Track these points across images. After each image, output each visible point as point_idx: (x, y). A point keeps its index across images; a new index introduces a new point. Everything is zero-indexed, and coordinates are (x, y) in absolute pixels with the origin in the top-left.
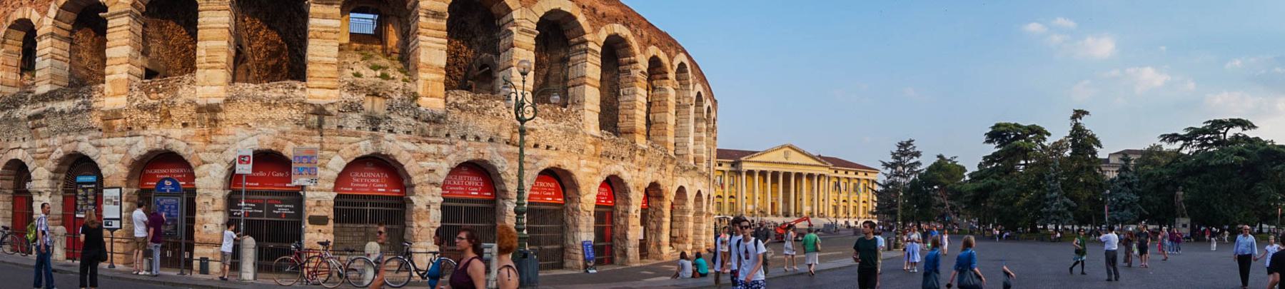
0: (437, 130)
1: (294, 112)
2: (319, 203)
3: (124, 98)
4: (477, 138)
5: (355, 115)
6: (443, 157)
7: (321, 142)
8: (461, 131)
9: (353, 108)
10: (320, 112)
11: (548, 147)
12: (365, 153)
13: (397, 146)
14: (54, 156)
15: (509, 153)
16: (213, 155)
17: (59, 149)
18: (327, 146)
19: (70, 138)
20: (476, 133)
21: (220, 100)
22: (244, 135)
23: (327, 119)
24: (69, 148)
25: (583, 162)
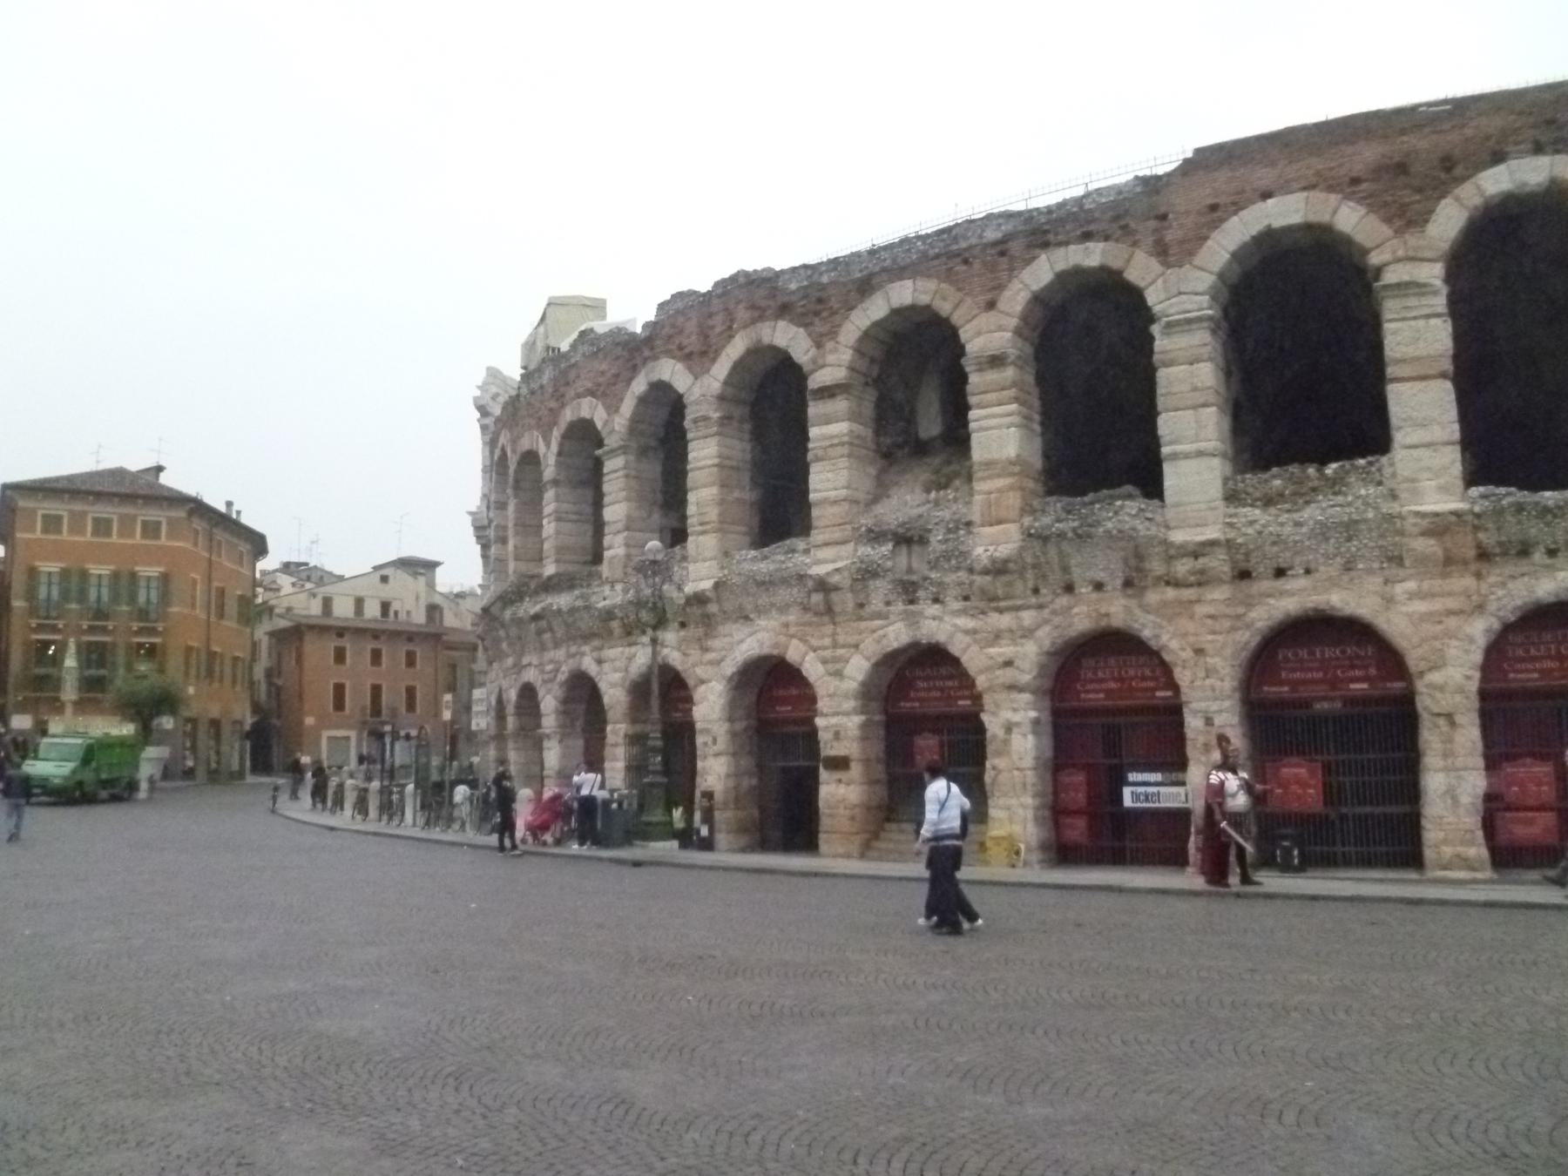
0: (1010, 584)
2: (837, 736)
4: (1099, 586)
5: (878, 583)
6: (1028, 633)
7: (834, 634)
8: (1056, 577)
9: (867, 573)
10: (823, 586)
11: (1280, 573)
12: (895, 645)
13: (942, 624)
14: (562, 677)
15: (1165, 604)
16: (709, 668)
17: (564, 668)
18: (841, 639)
19: (573, 649)
20: (1091, 574)
21: (707, 585)
23: (834, 597)
25: (1399, 589)
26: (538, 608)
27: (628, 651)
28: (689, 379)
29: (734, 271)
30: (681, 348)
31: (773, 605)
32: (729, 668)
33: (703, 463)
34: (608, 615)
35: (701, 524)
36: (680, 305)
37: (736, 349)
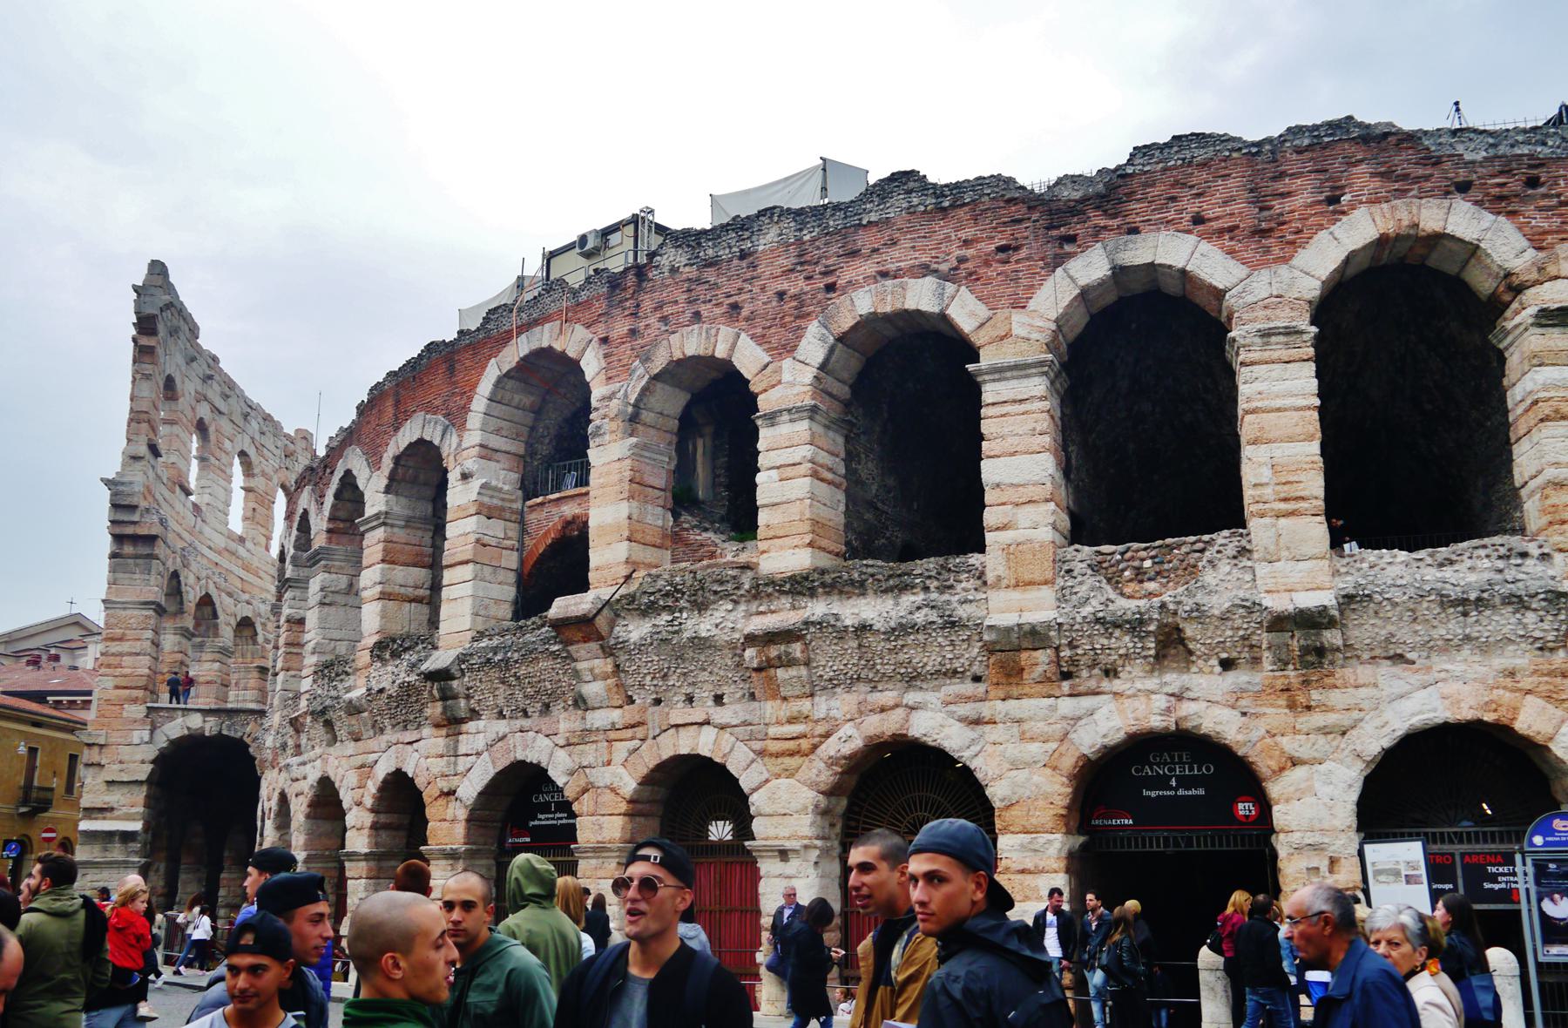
1: (1530, 617)
3: (1047, 594)
14: (831, 747)
16: (1321, 740)
17: (848, 729)
19: (887, 697)
22: (1399, 686)
24: (887, 725)
26: (758, 624)
27: (1067, 706)
28: (1239, 271)
29: (1337, 114)
30: (1198, 220)
31: (1467, 638)
32: (1376, 738)
33: (1288, 402)
34: (1034, 637)
35: (1285, 500)
36: (1201, 154)
37: (1358, 230)
